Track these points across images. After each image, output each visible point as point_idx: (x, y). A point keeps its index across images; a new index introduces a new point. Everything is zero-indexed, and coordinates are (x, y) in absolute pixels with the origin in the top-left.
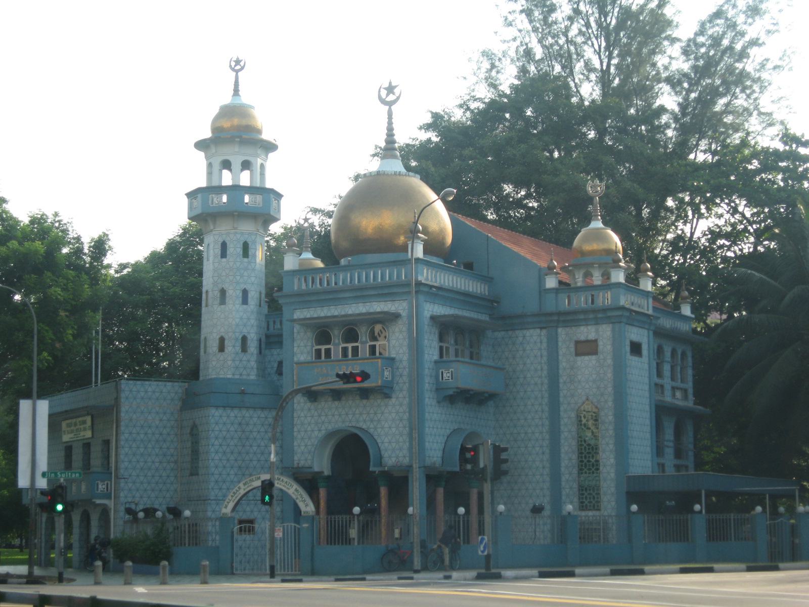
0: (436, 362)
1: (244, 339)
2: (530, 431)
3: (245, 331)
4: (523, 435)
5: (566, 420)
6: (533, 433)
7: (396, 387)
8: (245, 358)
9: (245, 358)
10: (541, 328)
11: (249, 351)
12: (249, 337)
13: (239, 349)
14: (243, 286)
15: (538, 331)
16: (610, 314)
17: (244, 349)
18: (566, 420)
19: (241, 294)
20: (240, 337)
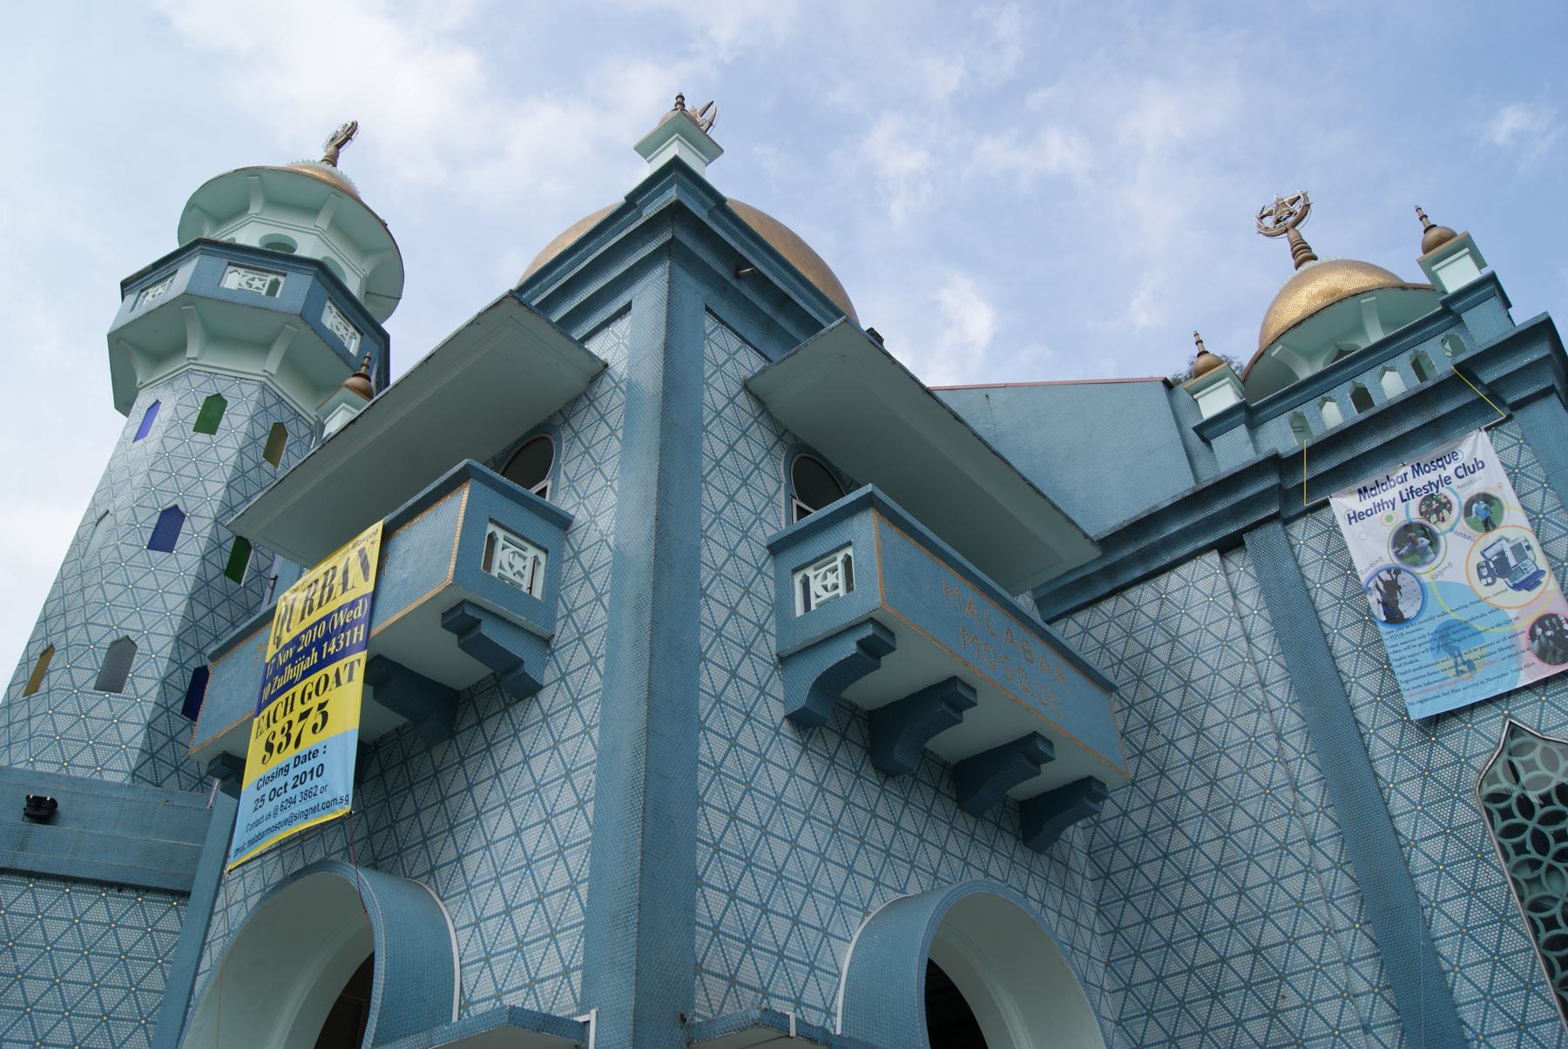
0: (777, 548)
1: (122, 653)
2: (1271, 935)
3: (131, 626)
4: (1242, 965)
5: (1434, 848)
6: (1291, 940)
7: (563, 633)
8: (103, 706)
9: (103, 710)
10: (1228, 546)
11: (128, 688)
12: (142, 645)
13: (86, 676)
14: (167, 502)
15: (1213, 558)
16: (1489, 376)
17: (112, 679)
18: (1434, 848)
19: (155, 520)
20: (108, 641)
